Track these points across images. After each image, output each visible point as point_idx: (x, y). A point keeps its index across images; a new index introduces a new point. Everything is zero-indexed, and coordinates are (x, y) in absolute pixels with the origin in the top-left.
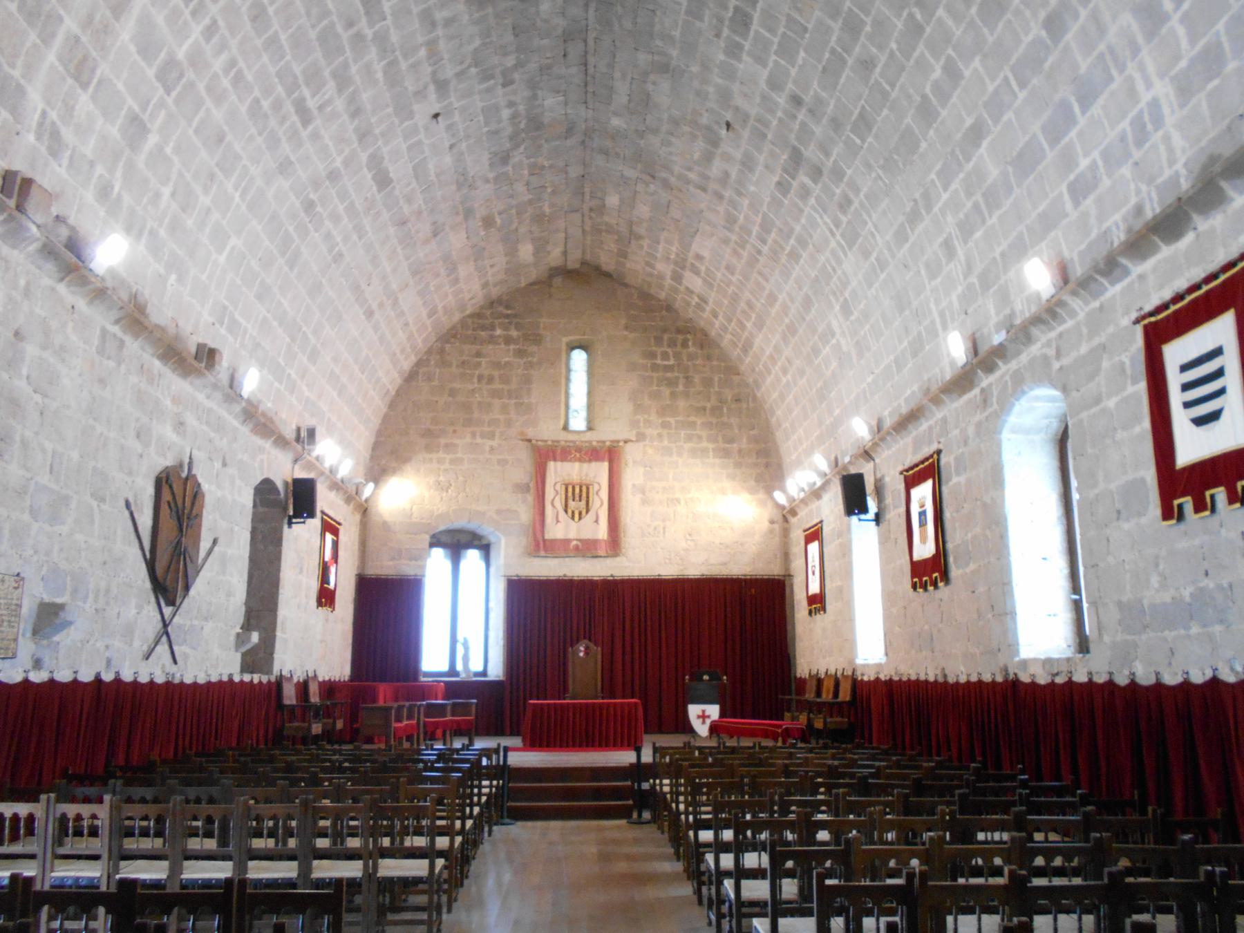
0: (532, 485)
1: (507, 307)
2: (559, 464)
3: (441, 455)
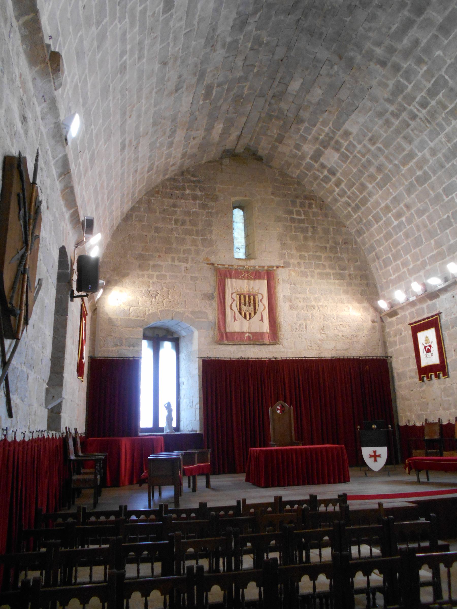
0: (215, 294)
1: (193, 176)
2: (234, 280)
3: (150, 272)
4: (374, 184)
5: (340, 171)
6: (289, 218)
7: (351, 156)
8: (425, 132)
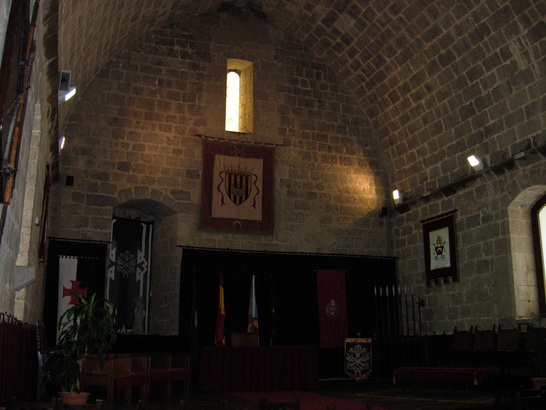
1: (184, 30)
4: (392, 59)
5: (356, 40)
6: (293, 88)
7: (369, 24)
8: (452, 8)
